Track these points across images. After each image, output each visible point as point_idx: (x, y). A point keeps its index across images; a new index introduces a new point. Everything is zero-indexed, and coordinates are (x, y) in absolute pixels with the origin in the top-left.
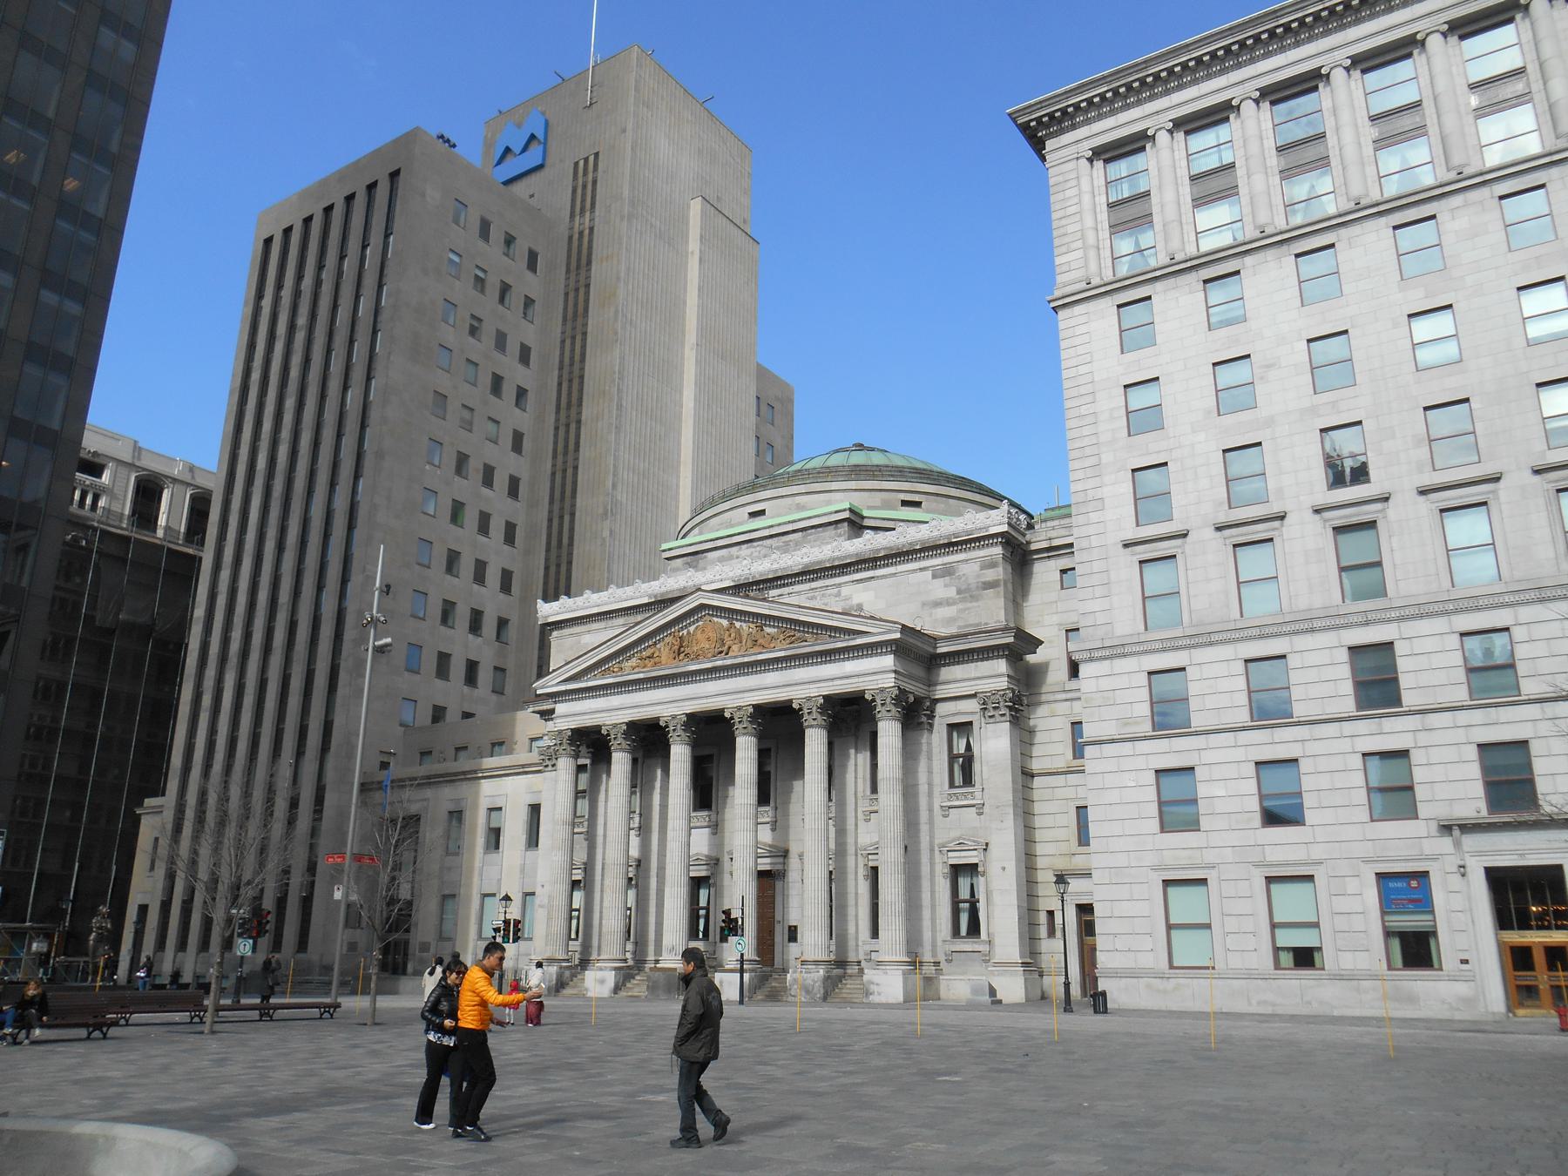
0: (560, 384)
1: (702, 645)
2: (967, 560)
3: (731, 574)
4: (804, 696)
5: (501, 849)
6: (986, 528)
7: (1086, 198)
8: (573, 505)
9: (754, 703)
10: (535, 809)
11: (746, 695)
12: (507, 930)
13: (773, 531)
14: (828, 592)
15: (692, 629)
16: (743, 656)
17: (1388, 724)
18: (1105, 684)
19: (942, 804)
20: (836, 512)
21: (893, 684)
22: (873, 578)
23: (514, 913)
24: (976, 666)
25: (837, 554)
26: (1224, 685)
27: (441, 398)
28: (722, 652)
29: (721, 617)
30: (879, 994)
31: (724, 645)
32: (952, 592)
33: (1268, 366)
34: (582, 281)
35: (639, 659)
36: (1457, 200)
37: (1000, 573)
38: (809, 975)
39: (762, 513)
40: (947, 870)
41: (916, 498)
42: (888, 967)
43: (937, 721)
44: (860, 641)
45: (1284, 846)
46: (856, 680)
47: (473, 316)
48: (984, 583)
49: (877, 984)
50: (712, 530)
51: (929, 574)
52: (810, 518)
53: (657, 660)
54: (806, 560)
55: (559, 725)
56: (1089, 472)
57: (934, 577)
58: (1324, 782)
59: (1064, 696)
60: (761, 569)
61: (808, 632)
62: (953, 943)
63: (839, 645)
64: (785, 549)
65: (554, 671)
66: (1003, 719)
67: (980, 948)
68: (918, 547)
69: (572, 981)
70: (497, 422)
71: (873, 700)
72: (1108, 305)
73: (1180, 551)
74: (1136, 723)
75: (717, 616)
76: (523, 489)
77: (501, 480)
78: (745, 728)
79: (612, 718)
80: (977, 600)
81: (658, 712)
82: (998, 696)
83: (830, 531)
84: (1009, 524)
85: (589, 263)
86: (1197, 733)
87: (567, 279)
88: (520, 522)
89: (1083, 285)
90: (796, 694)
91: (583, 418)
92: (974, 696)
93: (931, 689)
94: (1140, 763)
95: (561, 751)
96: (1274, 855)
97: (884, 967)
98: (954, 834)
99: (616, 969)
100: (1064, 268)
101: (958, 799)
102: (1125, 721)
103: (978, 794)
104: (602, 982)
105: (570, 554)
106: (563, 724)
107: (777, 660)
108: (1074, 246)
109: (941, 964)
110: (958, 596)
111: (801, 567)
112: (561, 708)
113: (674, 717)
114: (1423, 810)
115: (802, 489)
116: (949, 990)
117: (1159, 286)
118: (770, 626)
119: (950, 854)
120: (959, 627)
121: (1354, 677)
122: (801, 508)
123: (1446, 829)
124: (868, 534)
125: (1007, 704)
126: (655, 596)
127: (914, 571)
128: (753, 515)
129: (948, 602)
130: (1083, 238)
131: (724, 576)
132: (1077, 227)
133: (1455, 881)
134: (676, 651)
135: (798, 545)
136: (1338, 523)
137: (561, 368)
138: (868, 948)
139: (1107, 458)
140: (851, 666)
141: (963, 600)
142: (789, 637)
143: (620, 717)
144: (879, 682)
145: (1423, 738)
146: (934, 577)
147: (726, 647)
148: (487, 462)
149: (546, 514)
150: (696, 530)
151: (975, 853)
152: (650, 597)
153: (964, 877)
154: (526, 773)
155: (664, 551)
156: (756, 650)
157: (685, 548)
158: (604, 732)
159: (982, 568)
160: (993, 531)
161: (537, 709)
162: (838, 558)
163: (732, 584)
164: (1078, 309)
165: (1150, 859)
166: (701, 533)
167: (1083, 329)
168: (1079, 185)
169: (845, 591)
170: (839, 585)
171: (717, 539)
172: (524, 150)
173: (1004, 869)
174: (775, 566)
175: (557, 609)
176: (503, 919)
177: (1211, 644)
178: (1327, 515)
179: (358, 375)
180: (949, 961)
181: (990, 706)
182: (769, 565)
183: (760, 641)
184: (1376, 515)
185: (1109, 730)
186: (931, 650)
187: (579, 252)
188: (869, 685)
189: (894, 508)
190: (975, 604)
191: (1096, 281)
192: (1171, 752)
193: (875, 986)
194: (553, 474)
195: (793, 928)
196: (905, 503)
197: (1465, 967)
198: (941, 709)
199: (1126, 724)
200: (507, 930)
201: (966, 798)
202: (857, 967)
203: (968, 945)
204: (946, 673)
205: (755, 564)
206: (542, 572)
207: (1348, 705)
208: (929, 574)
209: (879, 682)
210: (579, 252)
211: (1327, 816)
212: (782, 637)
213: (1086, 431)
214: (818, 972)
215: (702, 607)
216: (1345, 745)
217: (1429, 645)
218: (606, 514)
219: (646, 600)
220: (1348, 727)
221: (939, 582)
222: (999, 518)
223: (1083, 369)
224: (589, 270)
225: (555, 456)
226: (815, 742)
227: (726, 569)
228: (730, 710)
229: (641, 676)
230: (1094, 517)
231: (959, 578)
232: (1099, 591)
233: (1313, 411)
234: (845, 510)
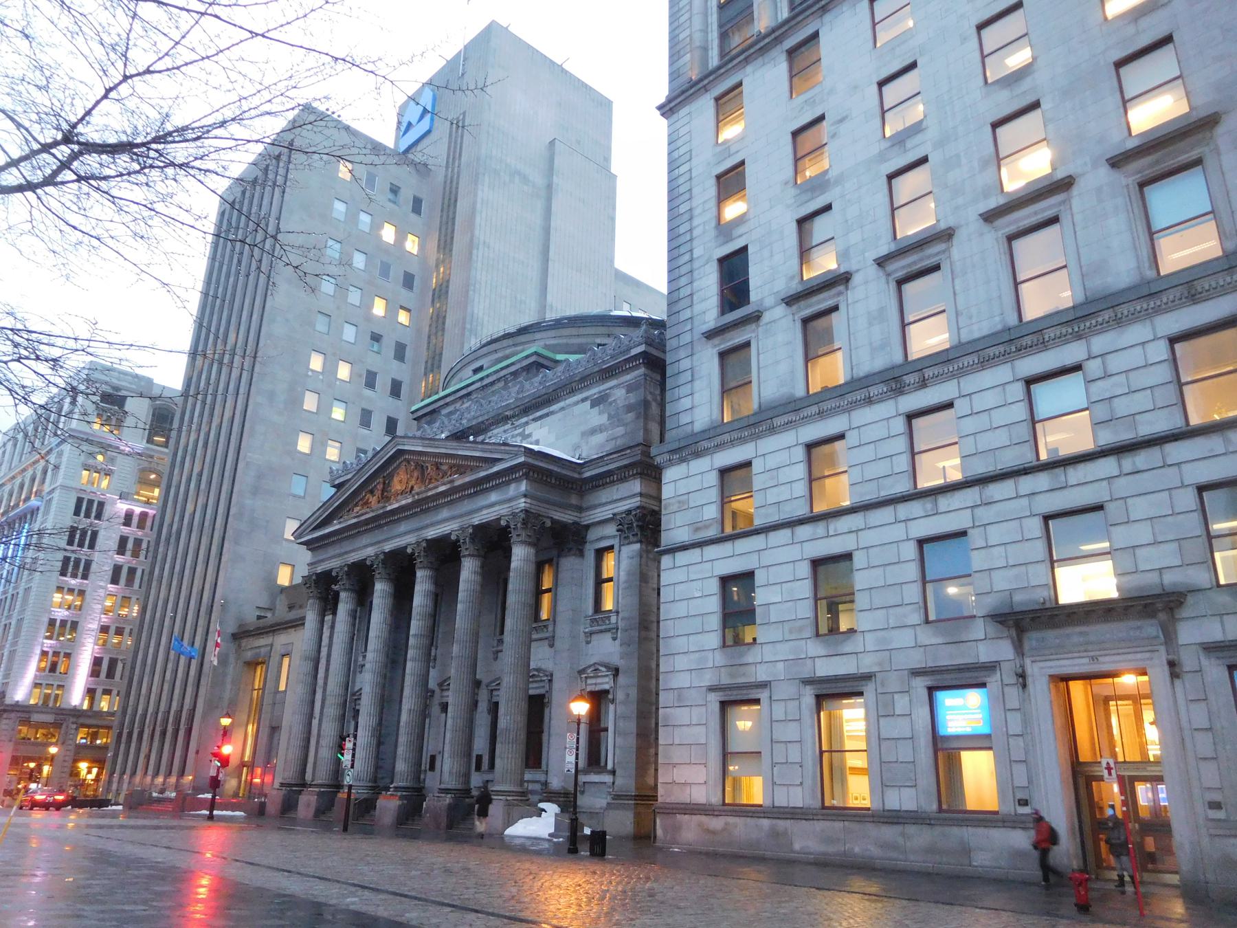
18: (683, 488)
34: (451, 216)
39: (481, 369)
43: (588, 546)
44: (495, 469)
51: (588, 403)
57: (592, 406)
63: (482, 474)
66: (635, 539)
73: (753, 335)
76: (404, 390)
77: (384, 383)
84: (646, 343)
85: (456, 201)
86: (757, 532)
87: (441, 216)
93: (583, 515)
119: (589, 681)
128: (476, 371)
145: (984, 514)
146: (592, 406)
148: (370, 369)
151: (606, 680)
155: (412, 413)
160: (634, 352)
167: (686, 129)
172: (420, 120)
184: (937, 258)
186: (576, 476)
187: (450, 193)
198: (592, 535)
199: (697, 530)
208: (588, 403)
210: (450, 193)
216: (898, 532)
217: (989, 400)
224: (455, 206)
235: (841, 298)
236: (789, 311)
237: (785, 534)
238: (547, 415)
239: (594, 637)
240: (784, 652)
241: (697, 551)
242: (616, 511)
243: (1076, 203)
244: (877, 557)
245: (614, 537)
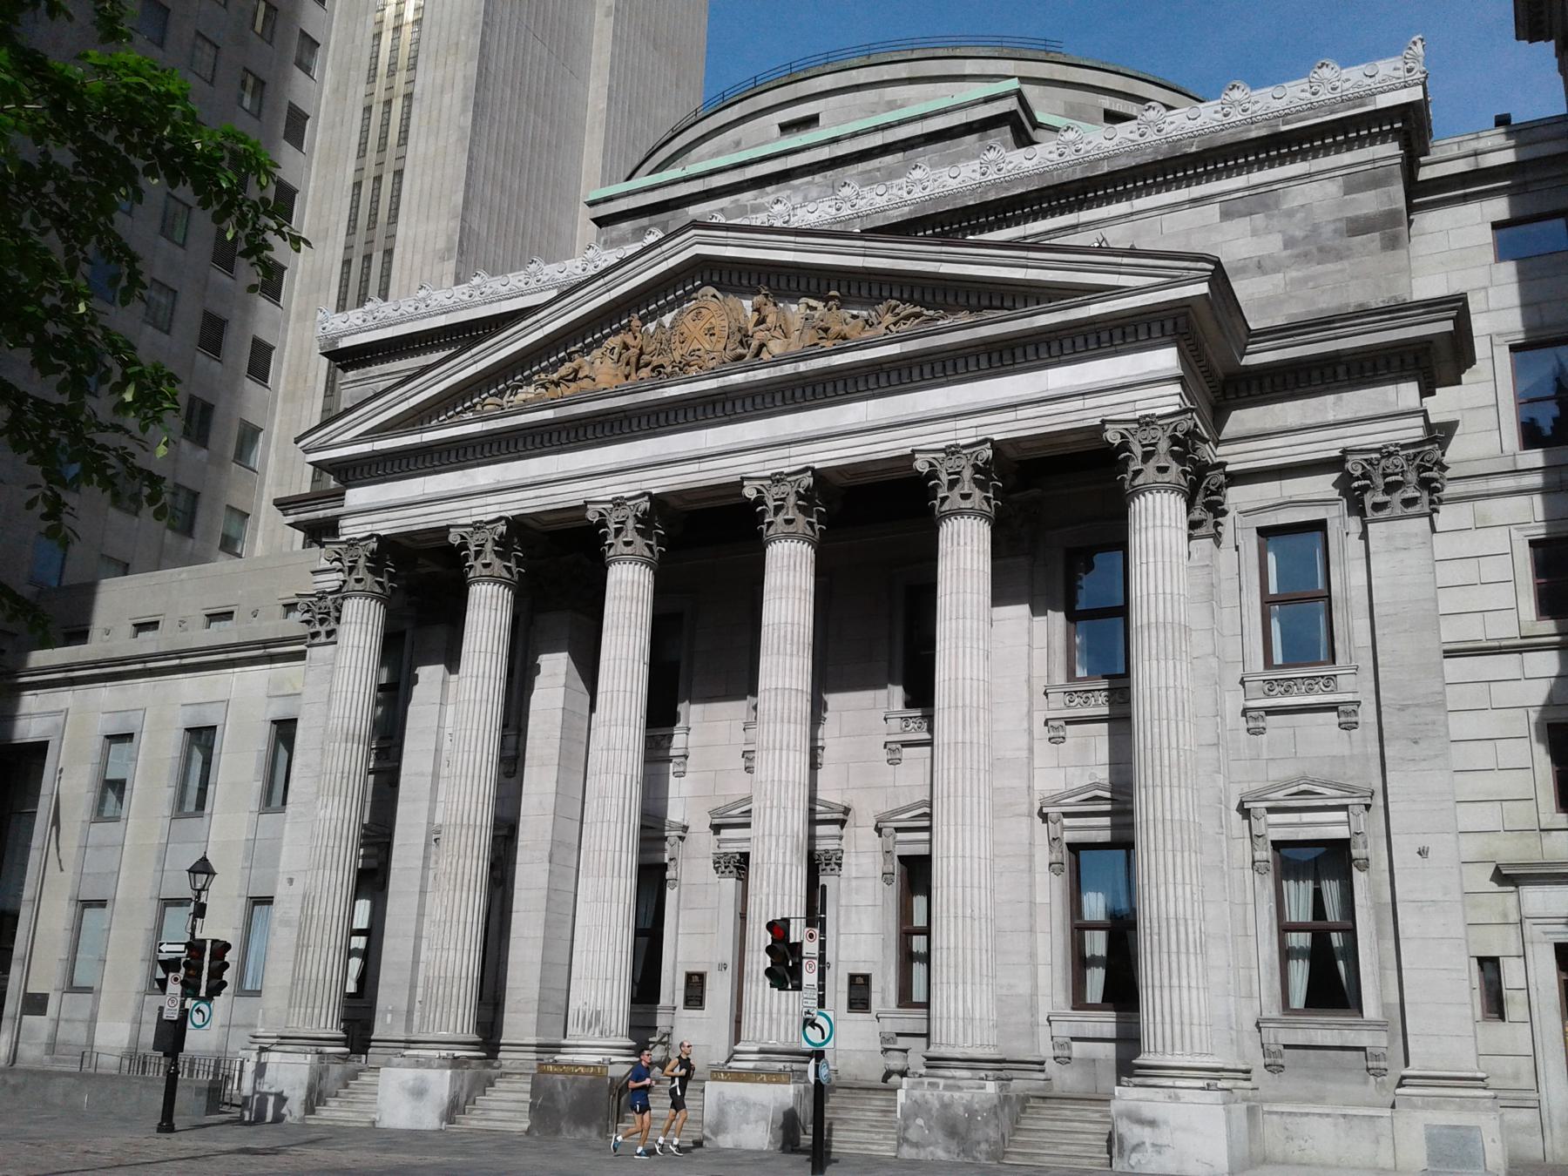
1: (696, 345)
2: (1310, 175)
4: (942, 446)
5: (207, 810)
9: (817, 466)
10: (285, 730)
11: (794, 450)
12: (194, 967)
15: (667, 319)
19: (1251, 704)
21: (1177, 408)
22: (1074, 226)
23: (220, 925)
24: (1340, 399)
25: (992, 176)
32: (1272, 244)
35: (543, 386)
38: (957, 1095)
39: (811, 121)
42: (1179, 1083)
44: (1096, 309)
46: (1077, 404)
49: (1152, 1123)
51: (1213, 210)
52: (924, 117)
54: (918, 193)
55: (351, 530)
57: (1226, 215)
64: (869, 180)
65: (348, 411)
67: (1364, 1038)
68: (1194, 149)
69: (346, 1086)
71: (1125, 446)
78: (789, 522)
79: (474, 511)
81: (584, 495)
82: (1400, 461)
91: (417, 90)
95: (352, 584)
97: (1169, 1082)
104: (419, 1092)
106: (361, 529)
109: (1254, 1075)
110: (1289, 252)
111: (907, 209)
113: (618, 502)
116: (1290, 1138)
122: (892, 105)
125: (1424, 475)
128: (785, 128)
134: (633, 360)
135: (892, 174)
141: (1305, 257)
142: (907, 318)
143: (490, 509)
144: (1139, 405)
146: (1226, 215)
147: (755, 343)
151: (1342, 815)
153: (1297, 880)
154: (272, 659)
155: (592, 204)
157: (639, 196)
159: (1350, 189)
160: (1384, 101)
162: (994, 185)
175: (359, 322)
176: (187, 939)
180: (1274, 1068)
181: (1380, 482)
182: (833, 211)
190: (1330, 267)
193: (1147, 1131)
194: (358, 185)
195: (860, 981)
200: (194, 967)
202: (1042, 1076)
203: (1326, 1030)
204: (1242, 420)
205: (798, 211)
209: (1139, 405)
214: (983, 1088)
218: (449, 250)
222: (1400, 73)
225: (362, 152)
228: (757, 483)
231: (1290, 214)
242: (1348, 443)
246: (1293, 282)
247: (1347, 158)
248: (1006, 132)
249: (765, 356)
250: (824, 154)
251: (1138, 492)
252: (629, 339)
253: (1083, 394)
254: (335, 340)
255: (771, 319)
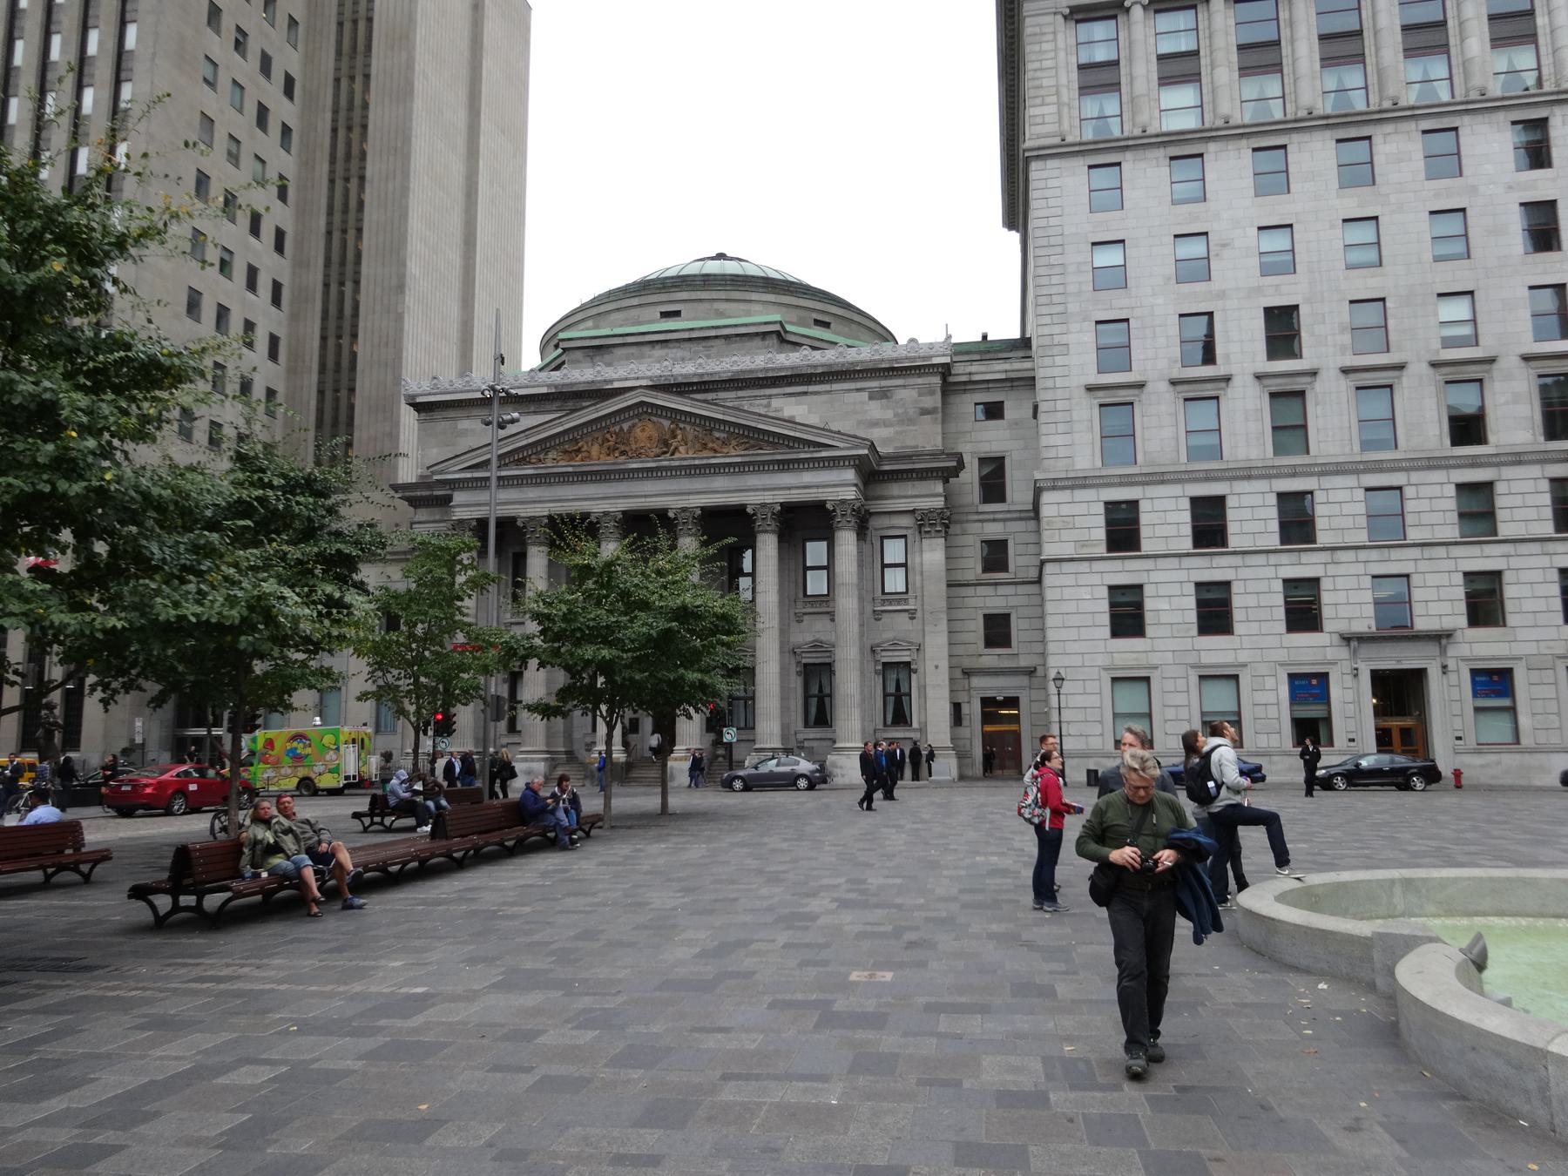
0: (334, 130)
3: (649, 374)
6: (930, 357)
7: (1062, 54)
8: (357, 273)
13: (695, 334)
14: (757, 402)
15: (626, 426)
16: (694, 458)
17: (1305, 557)
18: (1066, 510)
20: (766, 323)
26: (1172, 517)
27: (208, 121)
28: (665, 453)
29: (660, 416)
30: (843, 776)
31: (666, 444)
33: (1224, 246)
36: (1389, 128)
37: (935, 401)
40: (880, 667)
41: (827, 319)
44: (824, 454)
45: (1216, 651)
46: (815, 490)
47: (239, 29)
48: (922, 409)
50: (612, 326)
51: (865, 395)
52: (736, 326)
53: (585, 454)
56: (1056, 319)
57: (871, 398)
58: (1251, 601)
59: (976, 517)
60: (684, 371)
61: (762, 440)
62: (885, 731)
70: (263, 162)
71: (834, 511)
72: (1080, 164)
74: (1092, 546)
75: (656, 415)
80: (914, 424)
83: (757, 342)
88: (285, 281)
89: (1057, 140)
90: (751, 499)
92: (913, 511)
94: (1096, 579)
96: (1207, 659)
98: (888, 635)
99: (545, 760)
100: (1038, 120)
101: (891, 604)
102: (1084, 544)
103: (912, 601)
105: (355, 326)
107: (729, 465)
108: (1048, 100)
112: (459, 497)
114: (1328, 625)
115: (722, 295)
117: (1129, 155)
118: (719, 430)
119: (884, 654)
120: (896, 448)
121: (1280, 517)
123: (1347, 639)
124: (806, 351)
126: (556, 387)
127: (849, 390)
128: (665, 315)
129: (886, 423)
130: (1057, 93)
131: (640, 374)
132: (1052, 82)
133: (1349, 679)
136: (1274, 389)
137: (335, 111)
138: (801, 737)
139: (1073, 307)
140: (808, 477)
141: (901, 422)
145: (1332, 570)
146: (871, 398)
149: (320, 277)
150: (590, 323)
151: (908, 653)
152: (548, 386)
156: (705, 453)
158: (519, 523)
160: (936, 361)
161: (407, 494)
162: (773, 369)
163: (650, 383)
164: (1051, 163)
165: (1102, 660)
166: (596, 327)
168: (1055, 40)
169: (776, 403)
170: (770, 396)
171: (627, 335)
173: (937, 667)
174: (700, 371)
177: (1163, 482)
178: (1267, 382)
179: (102, 71)
183: (710, 445)
185: (1068, 550)
188: (830, 495)
189: (808, 326)
191: (1070, 139)
192: (1124, 571)
194: (329, 233)
196: (818, 323)
197: (1352, 744)
199: (1083, 546)
201: (899, 604)
206: (316, 343)
207: (1274, 540)
208: (865, 395)
211: (1254, 628)
212: (734, 443)
213: (1055, 280)
215: (642, 403)
216: (1270, 572)
217: (1341, 495)
219: (544, 390)
220: (1273, 558)
221: (875, 405)
223: (1053, 221)
225: (330, 213)
226: (768, 545)
227: (643, 367)
229: (570, 469)
230: (1059, 360)
232: (1061, 428)
233: (1258, 290)
234: (775, 322)
235: (1221, 392)
236: (1171, 388)
237: (1174, 562)
238: (805, 393)
239: (884, 615)
240: (1174, 644)
241: (1086, 564)
243: (1405, 380)
244: (1251, 586)
245: (907, 528)
246: (897, 433)
247: (919, 381)
248: (774, 340)
249: (677, 455)
250: (686, 335)
251: (839, 529)
252: (608, 436)
253: (818, 487)
254: (414, 397)
255: (679, 437)
